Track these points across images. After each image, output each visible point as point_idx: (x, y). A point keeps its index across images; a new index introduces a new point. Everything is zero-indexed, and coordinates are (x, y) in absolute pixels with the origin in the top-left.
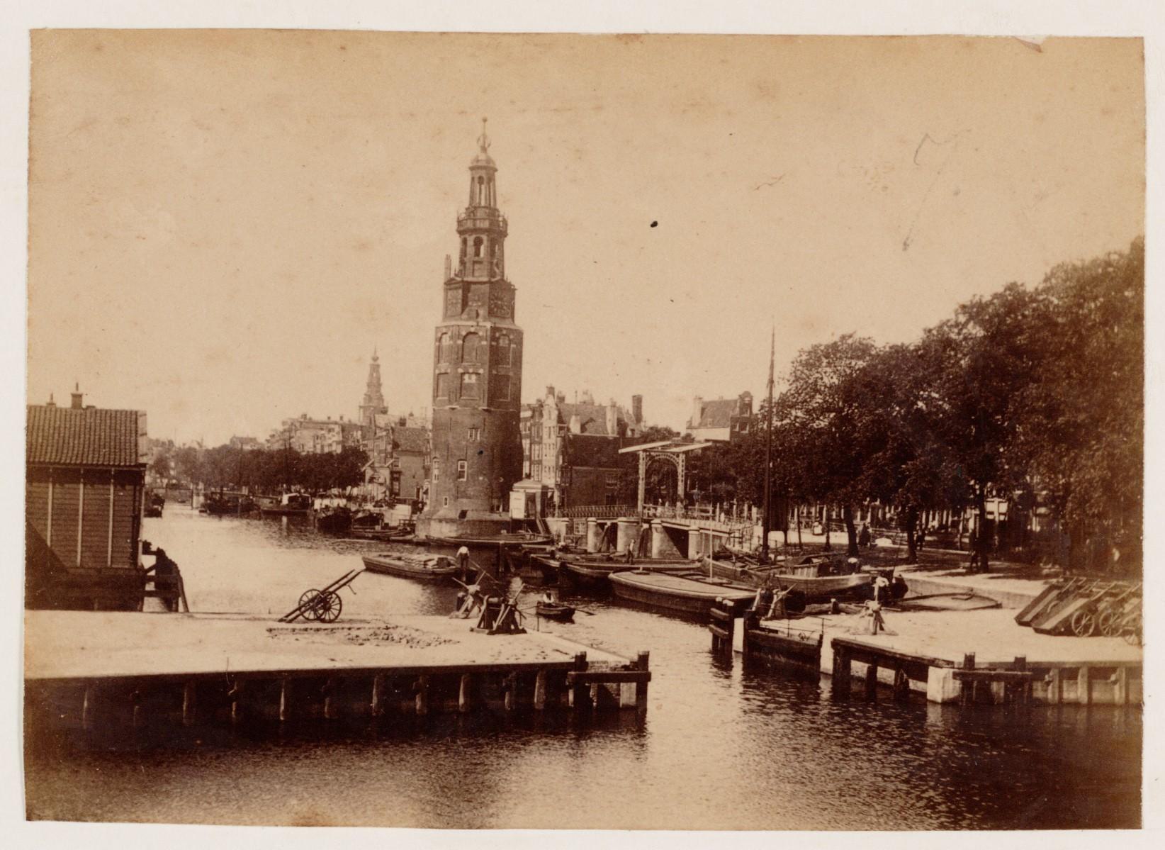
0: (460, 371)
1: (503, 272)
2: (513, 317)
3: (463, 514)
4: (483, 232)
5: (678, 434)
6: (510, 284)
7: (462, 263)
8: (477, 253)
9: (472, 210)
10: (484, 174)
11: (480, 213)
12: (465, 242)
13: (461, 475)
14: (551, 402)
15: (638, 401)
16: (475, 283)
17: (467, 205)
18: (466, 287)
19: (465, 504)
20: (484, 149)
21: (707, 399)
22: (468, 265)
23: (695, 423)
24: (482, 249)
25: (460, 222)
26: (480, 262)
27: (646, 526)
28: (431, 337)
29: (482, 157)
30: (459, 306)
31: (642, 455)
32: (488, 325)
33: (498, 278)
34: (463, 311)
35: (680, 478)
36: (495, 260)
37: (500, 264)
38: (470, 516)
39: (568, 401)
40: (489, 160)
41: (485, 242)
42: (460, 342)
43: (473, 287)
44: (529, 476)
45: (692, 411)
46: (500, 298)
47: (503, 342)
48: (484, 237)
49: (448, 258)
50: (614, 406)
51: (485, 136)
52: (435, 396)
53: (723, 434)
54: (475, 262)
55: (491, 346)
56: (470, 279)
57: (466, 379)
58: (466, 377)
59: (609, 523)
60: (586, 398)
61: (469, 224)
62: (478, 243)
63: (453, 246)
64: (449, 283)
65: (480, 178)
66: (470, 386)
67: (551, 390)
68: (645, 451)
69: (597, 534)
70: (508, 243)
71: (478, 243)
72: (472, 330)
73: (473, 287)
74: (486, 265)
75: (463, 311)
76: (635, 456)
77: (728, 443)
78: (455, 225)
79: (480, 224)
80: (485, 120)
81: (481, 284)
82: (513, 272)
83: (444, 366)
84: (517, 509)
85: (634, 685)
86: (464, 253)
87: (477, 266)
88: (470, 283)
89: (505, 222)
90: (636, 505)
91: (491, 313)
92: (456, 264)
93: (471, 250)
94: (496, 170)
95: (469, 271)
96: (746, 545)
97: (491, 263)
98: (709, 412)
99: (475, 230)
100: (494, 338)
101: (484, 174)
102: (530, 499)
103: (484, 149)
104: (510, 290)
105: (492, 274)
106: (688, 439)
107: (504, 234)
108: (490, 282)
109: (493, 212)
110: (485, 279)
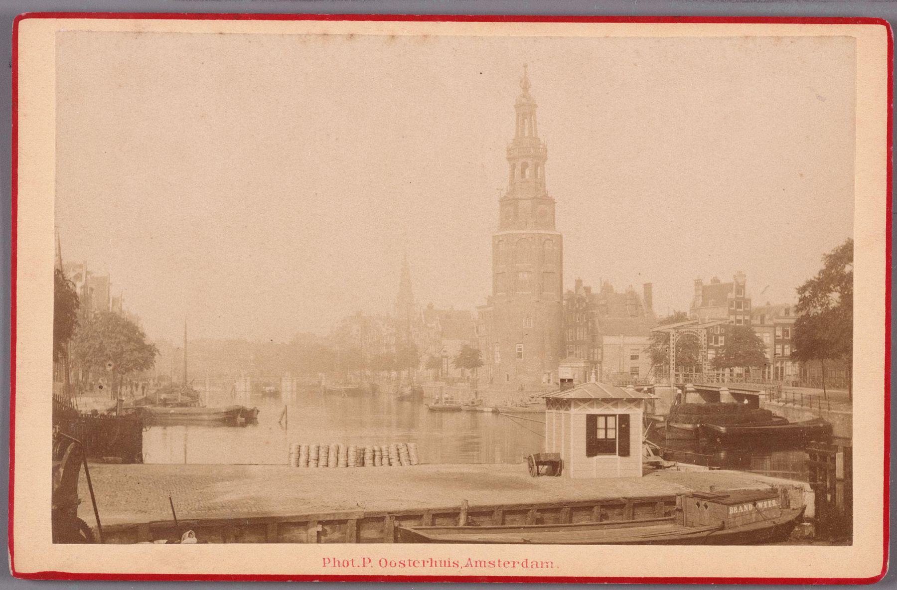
4: (527, 157)
10: (526, 110)
12: (513, 167)
15: (648, 287)
17: (513, 137)
20: (526, 88)
24: (527, 172)
25: (509, 150)
37: (542, 184)
48: (529, 161)
62: (525, 166)
71: (525, 166)
72: (524, 236)
81: (528, 201)
88: (517, 199)
93: (518, 172)
94: (536, 106)
101: (526, 110)
107: (544, 159)
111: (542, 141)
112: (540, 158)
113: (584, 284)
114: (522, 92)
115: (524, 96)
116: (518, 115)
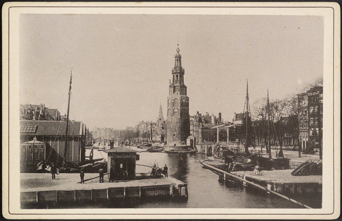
0: (173, 108)
1: (183, 83)
2: (186, 94)
3: (175, 145)
5: (230, 123)
6: (185, 86)
7: (173, 81)
8: (177, 79)
9: (176, 68)
10: (179, 58)
11: (178, 69)
12: (174, 76)
13: (174, 135)
14: (197, 115)
15: (220, 114)
16: (176, 86)
18: (174, 87)
19: (175, 142)
20: (178, 52)
21: (237, 113)
22: (175, 82)
23: (235, 119)
24: (178, 78)
25: (172, 71)
26: (178, 81)
27: (218, 147)
28: (166, 100)
29: (178, 54)
30: (173, 92)
31: (218, 129)
32: (180, 96)
33: (182, 84)
34: (174, 93)
35: (228, 134)
36: (182, 80)
37: (183, 81)
38: (176, 146)
39: (202, 115)
40: (179, 55)
41: (179, 76)
42: (173, 101)
43: (176, 87)
44: (191, 135)
45: (234, 116)
46: (183, 89)
47: (184, 100)
48: (179, 74)
49: (170, 80)
50: (213, 115)
51: (178, 49)
52: (168, 115)
53: (240, 122)
54: (176, 81)
55: (181, 102)
56: (176, 85)
57: (175, 111)
58: (175, 110)
59: (209, 146)
60: (207, 114)
61: (175, 71)
62: (177, 76)
63: (171, 77)
64: (170, 86)
65: (177, 60)
66: (176, 112)
67: (198, 112)
68: (218, 127)
69: (207, 149)
70: (185, 76)
72: (176, 98)
73: (176, 87)
74: (179, 81)
75: (174, 93)
76: (216, 129)
77: (242, 124)
78: (171, 72)
79: (178, 72)
80: (178, 45)
82: (186, 83)
83: (170, 107)
84: (188, 143)
85: (85, 174)
86: (174, 79)
87: (177, 82)
89: (184, 71)
90: (216, 141)
91: (181, 94)
92: (172, 82)
93: (176, 78)
95: (175, 83)
96: (242, 150)
97: (180, 81)
98: (237, 116)
99: (175, 73)
100: (181, 100)
102: (191, 140)
103: (178, 52)
104: (185, 87)
105: (180, 83)
106: (232, 124)
108: (180, 86)
109: (181, 68)
110: (179, 85)
111: (183, 68)
112: (181, 73)
113: (199, 113)
114: (176, 53)
115: (178, 54)
116: (175, 60)
